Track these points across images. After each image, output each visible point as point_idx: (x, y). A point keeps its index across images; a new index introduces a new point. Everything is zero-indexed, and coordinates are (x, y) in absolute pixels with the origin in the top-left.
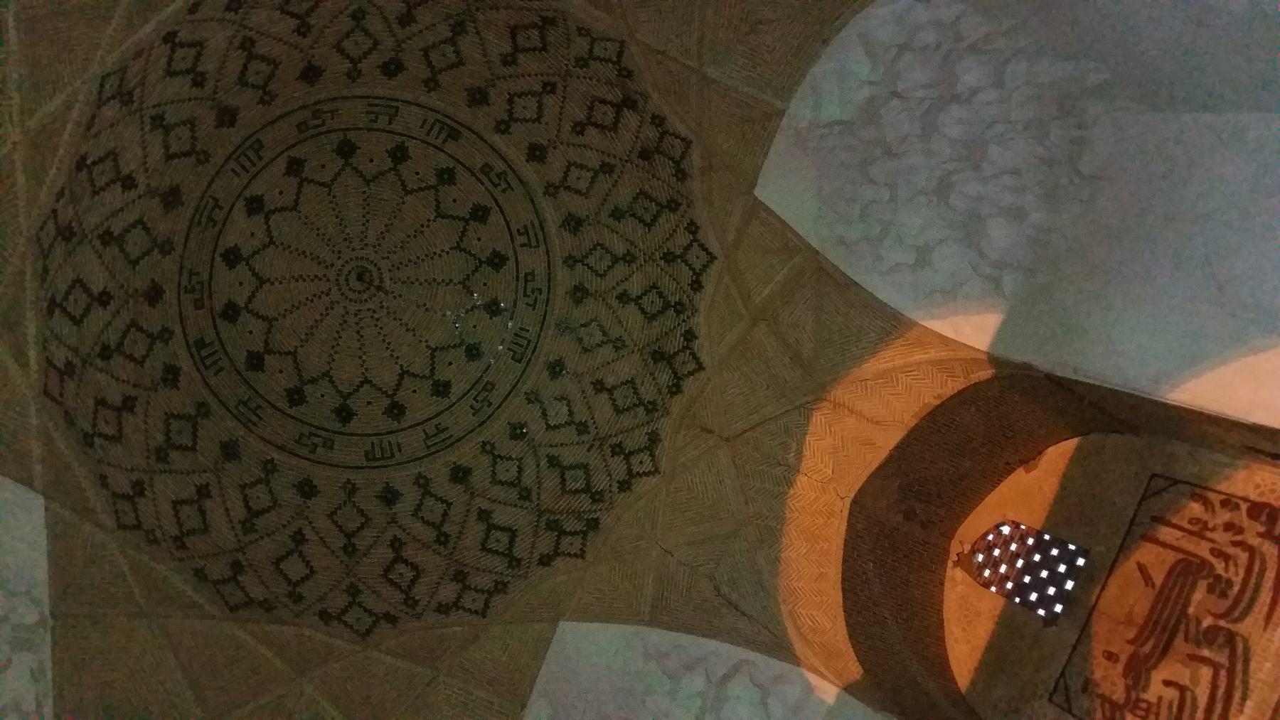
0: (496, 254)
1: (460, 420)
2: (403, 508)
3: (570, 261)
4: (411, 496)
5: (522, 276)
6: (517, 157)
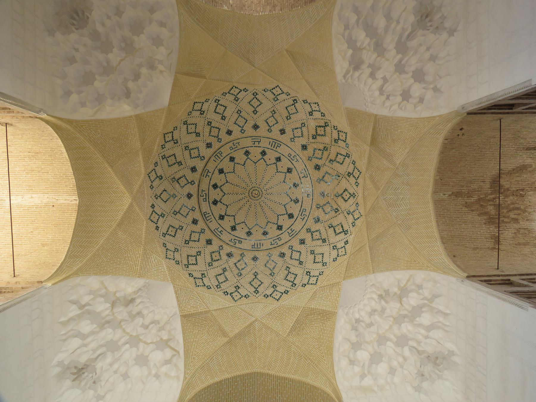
1: (226, 237)
4: (197, 228)
5: (279, 237)
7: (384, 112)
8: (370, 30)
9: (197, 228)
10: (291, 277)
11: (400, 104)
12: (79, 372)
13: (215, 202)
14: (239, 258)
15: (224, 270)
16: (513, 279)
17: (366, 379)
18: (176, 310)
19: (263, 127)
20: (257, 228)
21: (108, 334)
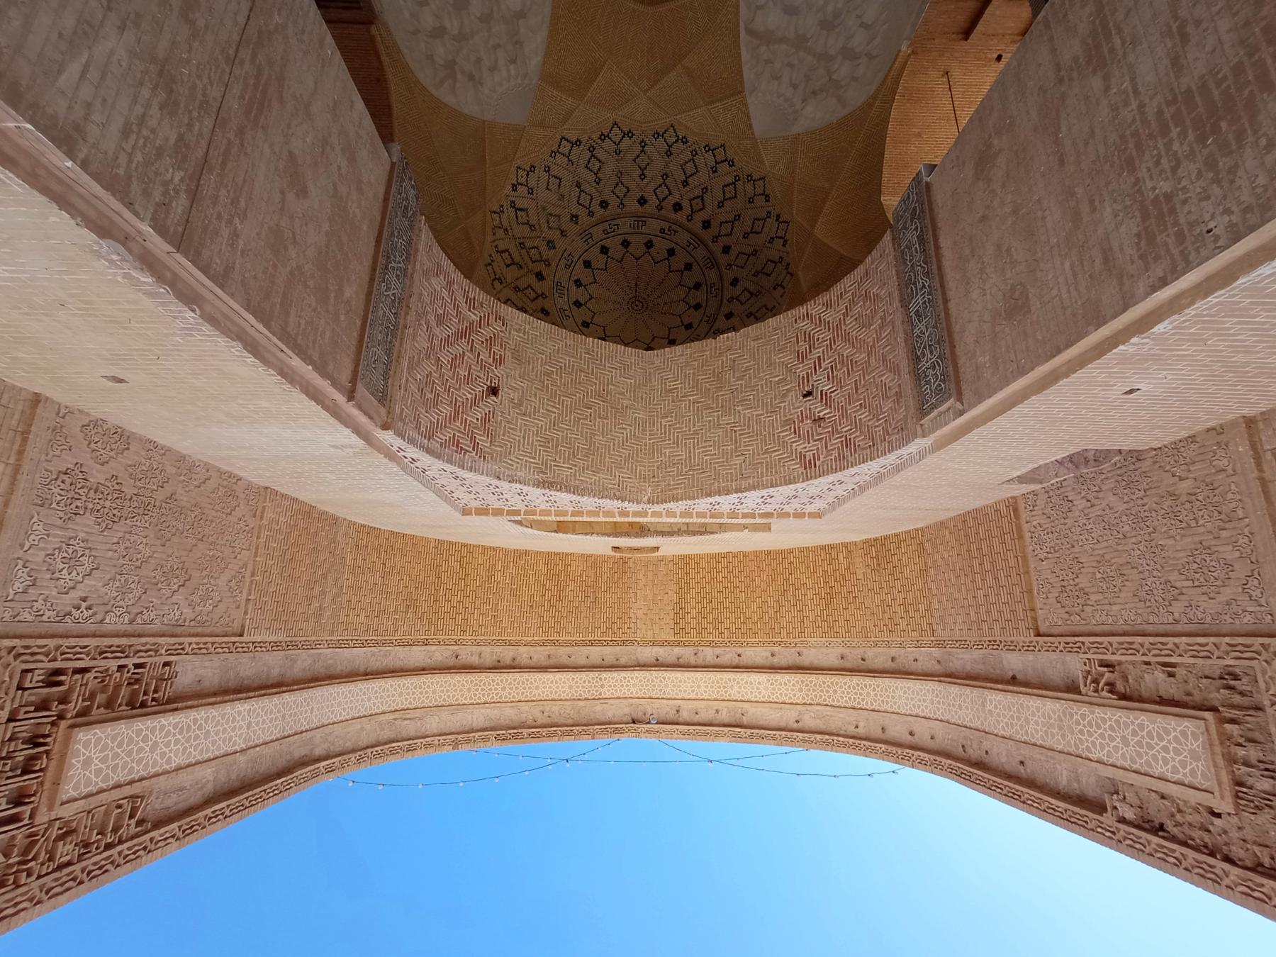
0: (602, 252)
9: (724, 241)
10: (594, 165)
13: (697, 286)
14: (664, 204)
15: (685, 183)
18: (751, 100)
20: (638, 254)
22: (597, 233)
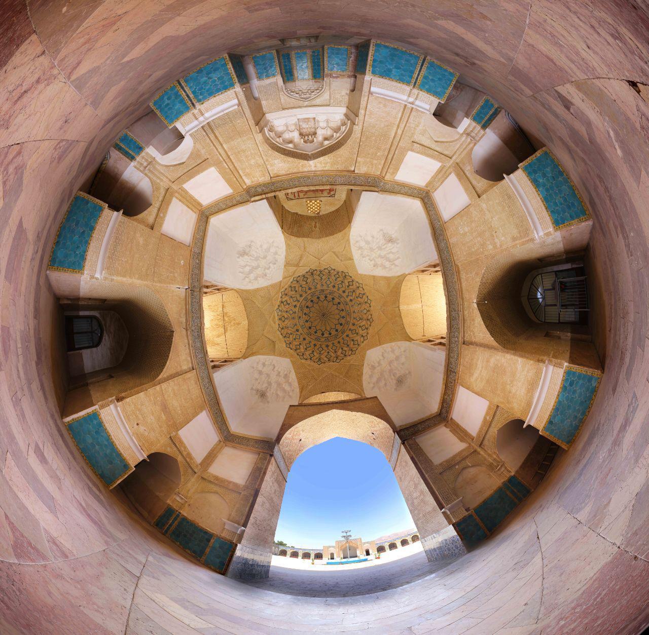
1: (336, 295)
2: (352, 298)
3: (306, 293)
4: (350, 298)
6: (297, 308)
7: (272, 357)
8: (284, 390)
9: (350, 298)
11: (266, 361)
12: (390, 240)
16: (218, 291)
17: (272, 241)
19: (324, 346)
21: (383, 253)
22: (309, 297)
